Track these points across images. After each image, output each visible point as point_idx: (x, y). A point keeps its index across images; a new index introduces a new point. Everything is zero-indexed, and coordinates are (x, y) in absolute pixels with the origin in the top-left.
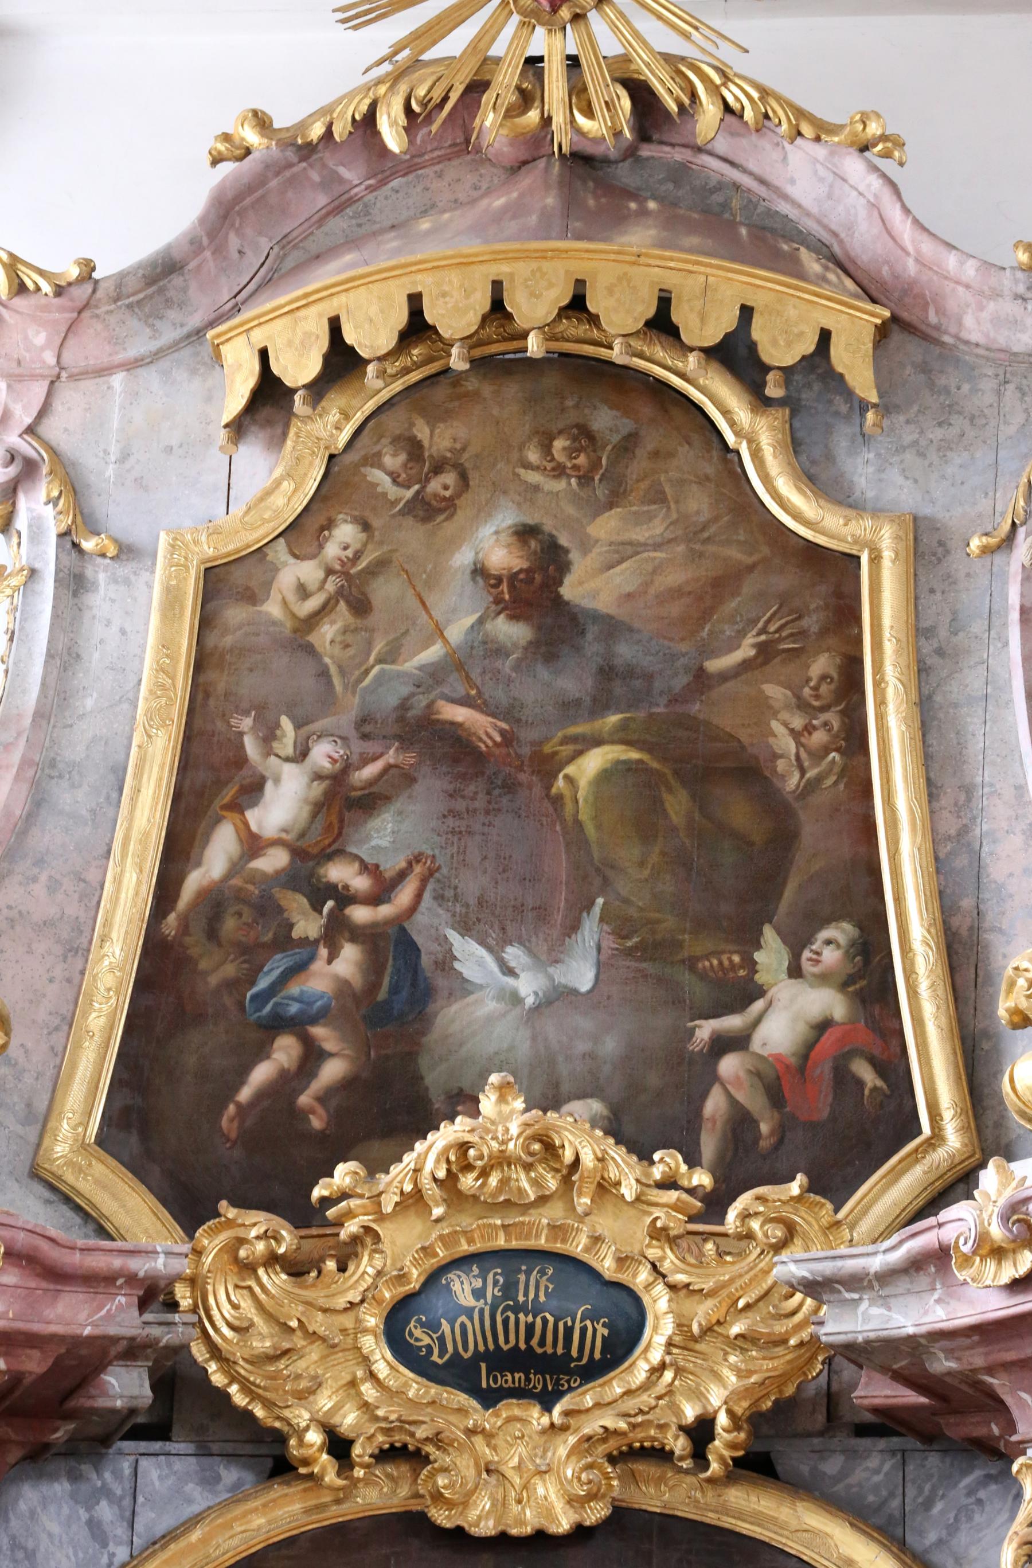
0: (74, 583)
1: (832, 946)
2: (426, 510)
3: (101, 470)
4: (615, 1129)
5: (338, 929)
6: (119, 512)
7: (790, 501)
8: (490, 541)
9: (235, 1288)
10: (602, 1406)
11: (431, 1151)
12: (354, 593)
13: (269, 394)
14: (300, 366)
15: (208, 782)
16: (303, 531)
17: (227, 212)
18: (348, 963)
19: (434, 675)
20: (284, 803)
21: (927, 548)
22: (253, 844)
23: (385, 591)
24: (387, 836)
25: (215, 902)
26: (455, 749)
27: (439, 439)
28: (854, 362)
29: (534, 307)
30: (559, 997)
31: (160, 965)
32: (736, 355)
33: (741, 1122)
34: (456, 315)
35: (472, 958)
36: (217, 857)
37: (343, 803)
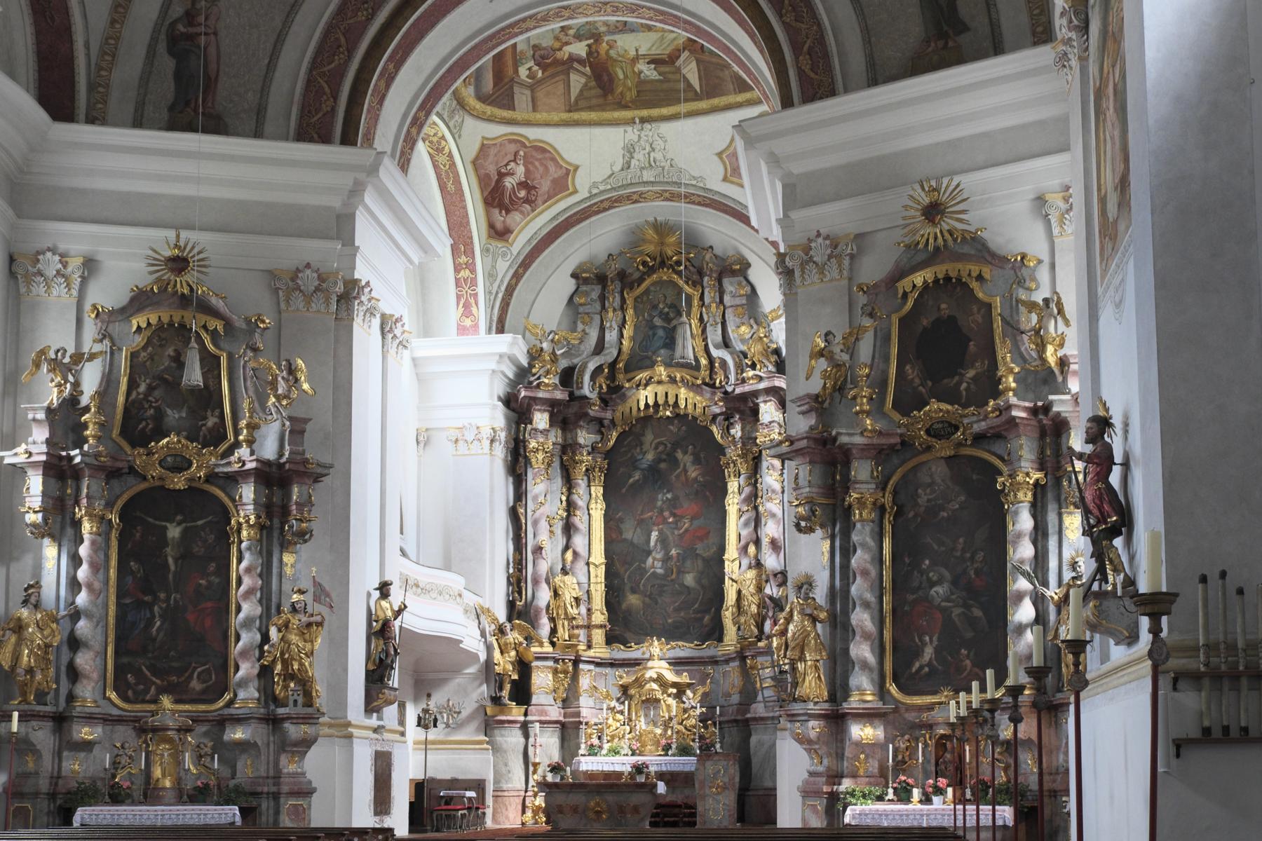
0: (112, 353)
1: (217, 412)
2: (161, 346)
3: (115, 336)
4: (187, 438)
5: (151, 407)
6: (117, 342)
7: (211, 347)
8: (170, 351)
9: (138, 458)
10: (186, 474)
11: (165, 441)
12: (151, 358)
13: (139, 328)
14: (144, 325)
15: (132, 385)
16: (144, 348)
17: (132, 300)
18: (152, 411)
19: (163, 371)
20: (142, 388)
21: (231, 357)
22: (138, 394)
23: (156, 358)
24: (157, 393)
25: (134, 402)
26: (166, 381)
27: (163, 336)
28: (220, 328)
29: (176, 319)
30: (181, 418)
31: (127, 410)
32: (205, 327)
33: (205, 436)
34: (165, 320)
35: (169, 412)
36: (134, 395)
37: (151, 389)
